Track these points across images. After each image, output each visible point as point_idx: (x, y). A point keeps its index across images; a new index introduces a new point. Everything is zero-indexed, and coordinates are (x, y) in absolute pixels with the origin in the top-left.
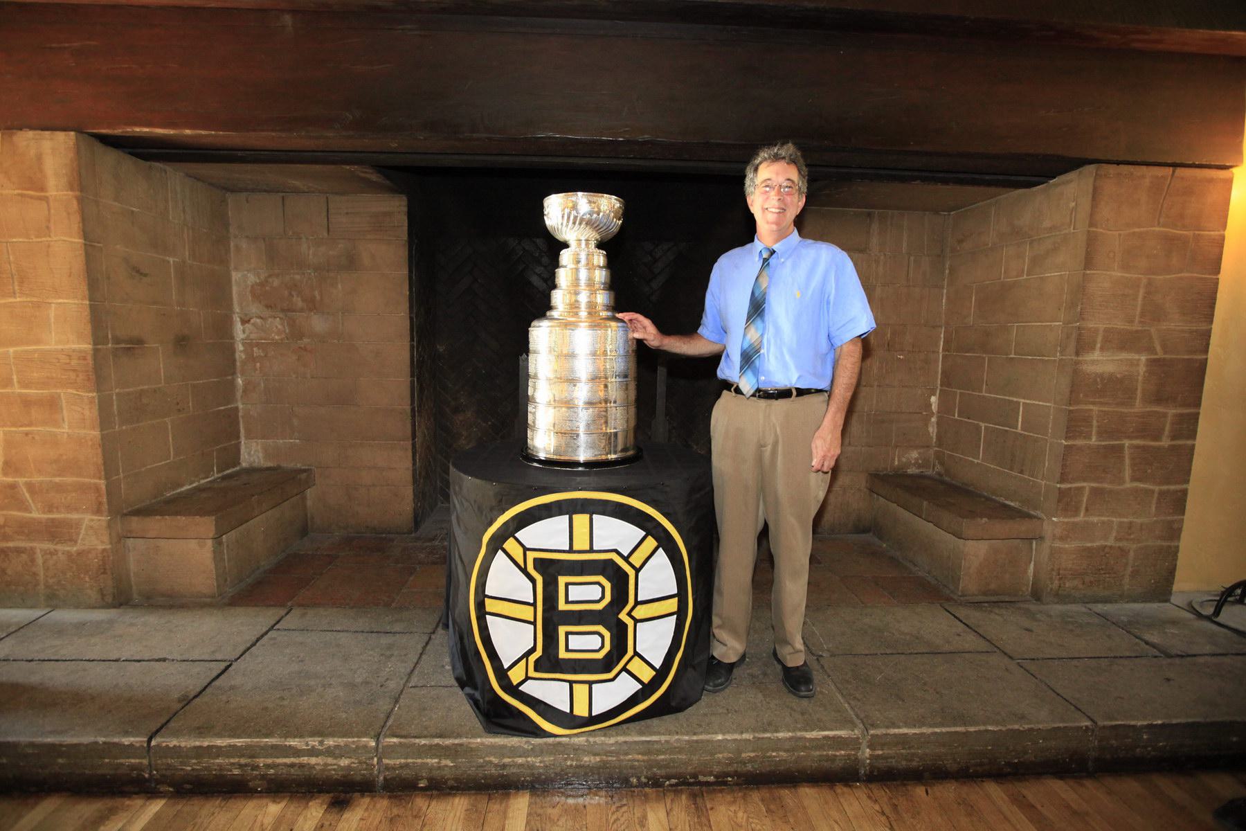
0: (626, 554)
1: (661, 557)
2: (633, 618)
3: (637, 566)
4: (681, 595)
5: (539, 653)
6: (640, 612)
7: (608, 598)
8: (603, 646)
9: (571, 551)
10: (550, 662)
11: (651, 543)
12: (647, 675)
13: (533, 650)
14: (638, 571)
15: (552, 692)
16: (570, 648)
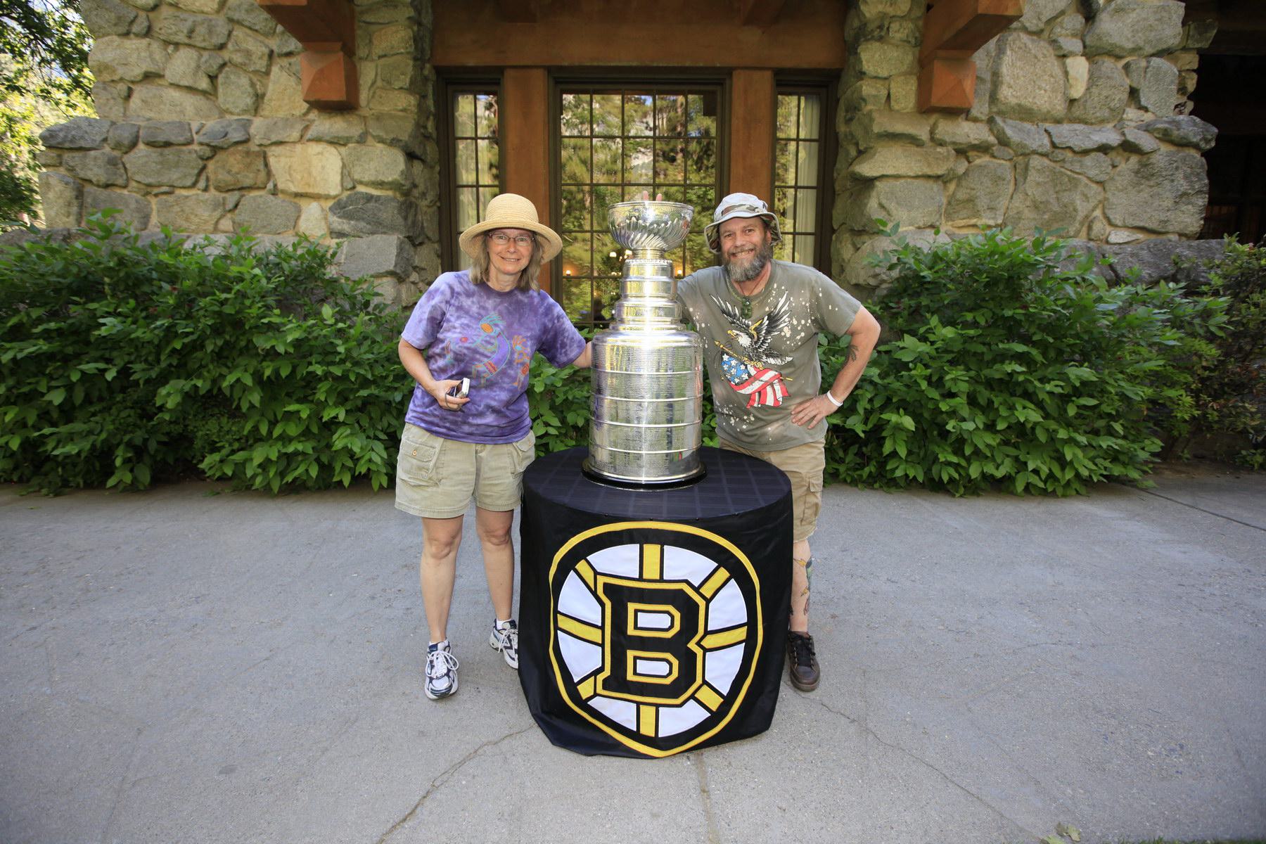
0: (696, 586)
1: (733, 588)
2: (702, 647)
3: (708, 596)
4: (751, 624)
5: (607, 672)
6: (709, 642)
7: (677, 627)
8: (670, 673)
9: (641, 579)
10: (617, 683)
11: (723, 574)
12: (714, 702)
13: (601, 669)
14: (708, 601)
15: (620, 710)
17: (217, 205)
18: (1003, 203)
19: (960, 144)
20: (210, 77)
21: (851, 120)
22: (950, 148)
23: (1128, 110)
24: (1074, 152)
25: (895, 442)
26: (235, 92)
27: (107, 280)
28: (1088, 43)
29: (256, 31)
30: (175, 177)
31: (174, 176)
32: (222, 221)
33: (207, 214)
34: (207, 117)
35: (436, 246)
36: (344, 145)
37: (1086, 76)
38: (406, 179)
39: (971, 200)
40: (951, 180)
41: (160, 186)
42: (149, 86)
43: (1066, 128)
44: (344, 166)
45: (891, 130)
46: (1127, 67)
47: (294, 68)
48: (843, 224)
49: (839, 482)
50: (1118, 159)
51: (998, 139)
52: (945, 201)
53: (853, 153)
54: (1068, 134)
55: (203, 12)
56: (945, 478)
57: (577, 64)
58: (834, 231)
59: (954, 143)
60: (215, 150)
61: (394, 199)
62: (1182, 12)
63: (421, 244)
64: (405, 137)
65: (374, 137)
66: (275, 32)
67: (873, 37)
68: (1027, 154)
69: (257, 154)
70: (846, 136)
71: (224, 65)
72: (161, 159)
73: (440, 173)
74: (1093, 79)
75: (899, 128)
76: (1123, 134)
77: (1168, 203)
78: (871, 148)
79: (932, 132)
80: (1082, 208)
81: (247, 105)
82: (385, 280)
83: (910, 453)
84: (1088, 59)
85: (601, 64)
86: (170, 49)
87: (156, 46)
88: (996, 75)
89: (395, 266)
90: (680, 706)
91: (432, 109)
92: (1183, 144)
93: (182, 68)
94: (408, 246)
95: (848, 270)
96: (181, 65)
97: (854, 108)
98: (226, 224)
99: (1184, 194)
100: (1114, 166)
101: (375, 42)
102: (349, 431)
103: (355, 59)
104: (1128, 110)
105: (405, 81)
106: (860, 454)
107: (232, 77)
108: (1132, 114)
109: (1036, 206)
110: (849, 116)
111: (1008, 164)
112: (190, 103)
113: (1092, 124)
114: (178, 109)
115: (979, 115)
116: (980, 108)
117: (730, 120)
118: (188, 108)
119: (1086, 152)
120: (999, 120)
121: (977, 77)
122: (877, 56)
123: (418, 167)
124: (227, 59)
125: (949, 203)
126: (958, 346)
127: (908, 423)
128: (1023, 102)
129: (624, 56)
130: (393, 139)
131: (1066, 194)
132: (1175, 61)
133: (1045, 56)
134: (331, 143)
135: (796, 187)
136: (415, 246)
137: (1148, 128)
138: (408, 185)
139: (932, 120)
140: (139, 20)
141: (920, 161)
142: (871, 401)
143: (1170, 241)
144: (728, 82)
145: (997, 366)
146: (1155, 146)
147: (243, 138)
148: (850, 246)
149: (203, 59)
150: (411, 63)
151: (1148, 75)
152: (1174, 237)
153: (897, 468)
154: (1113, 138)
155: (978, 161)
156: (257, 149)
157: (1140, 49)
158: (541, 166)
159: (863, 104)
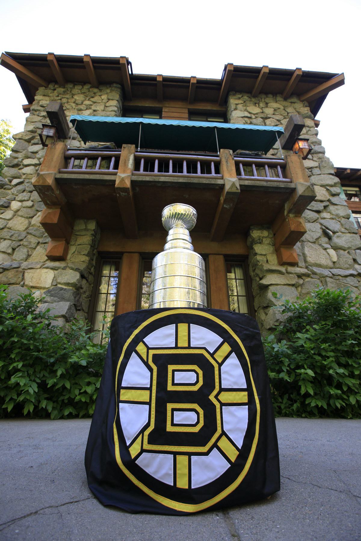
0: (212, 352)
4: (249, 389)
7: (201, 383)
11: (226, 348)
16: (175, 422)
19: (298, 273)
21: (255, 270)
24: (342, 276)
25: (306, 387)
26: (20, 254)
28: (332, 244)
29: (36, 236)
35: (86, 314)
36: (57, 270)
37: (336, 255)
38: (79, 282)
40: (298, 286)
44: (54, 277)
47: (45, 247)
48: (259, 307)
49: (283, 416)
53: (258, 279)
54: (335, 271)
55: (19, 231)
56: (339, 406)
57: (151, 252)
58: (256, 311)
61: (71, 290)
63: (79, 310)
65: (69, 267)
66: (42, 237)
67: (257, 243)
69: (21, 272)
70: (254, 275)
71: (20, 245)
73: (93, 287)
74: (338, 256)
75: (274, 268)
76: (357, 271)
78: (265, 276)
79: (286, 270)
81: (23, 258)
82: (60, 319)
83: (315, 394)
84: (334, 250)
89: (66, 313)
90: (207, 454)
91: (94, 264)
94: (73, 308)
95: (265, 323)
97: (255, 265)
101: (78, 240)
102: (21, 375)
103: (69, 245)
104: (355, 265)
105: (86, 252)
106: (290, 399)
108: (357, 266)
110: (254, 268)
111: (318, 280)
113: (344, 269)
115: (302, 266)
116: (301, 263)
119: (346, 276)
123: (84, 281)
124: (21, 244)
125: (300, 295)
126: (322, 337)
127: (310, 373)
128: (317, 262)
130: (77, 268)
133: (319, 249)
136: (77, 310)
138: (79, 285)
139: (286, 266)
141: (284, 279)
142: (289, 366)
144: (207, 259)
145: (344, 343)
148: (264, 314)
149: (13, 244)
150: (90, 247)
151: (357, 255)
153: (311, 402)
154: (355, 273)
155: (307, 280)
156: (22, 270)
157: (351, 248)
158: (134, 285)
159: (258, 263)
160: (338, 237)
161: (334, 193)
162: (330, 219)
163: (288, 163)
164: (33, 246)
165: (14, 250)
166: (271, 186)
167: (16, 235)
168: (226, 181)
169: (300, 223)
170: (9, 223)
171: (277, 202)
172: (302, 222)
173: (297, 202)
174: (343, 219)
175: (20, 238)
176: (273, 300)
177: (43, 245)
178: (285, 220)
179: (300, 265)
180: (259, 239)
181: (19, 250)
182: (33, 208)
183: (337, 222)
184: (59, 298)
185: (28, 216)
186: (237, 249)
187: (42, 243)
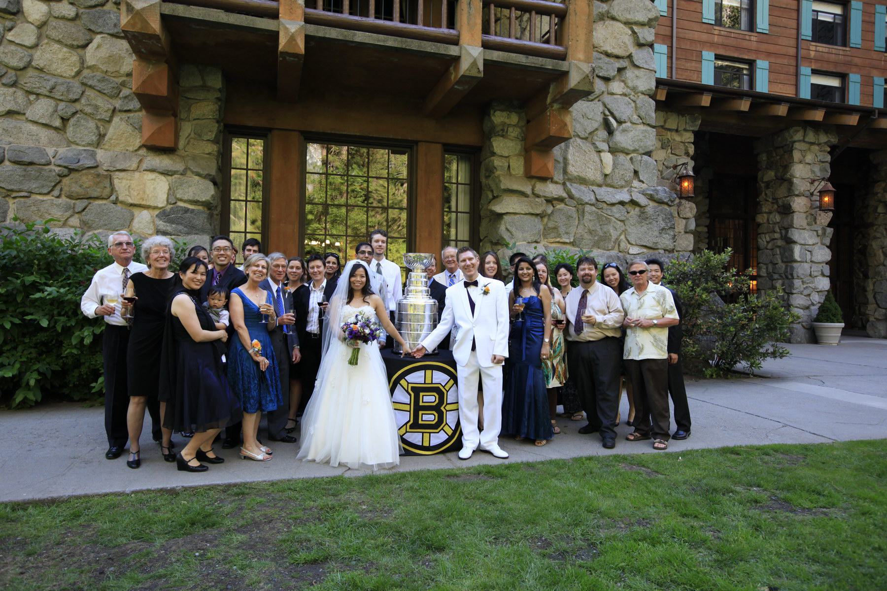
17: (68, 208)
18: (573, 230)
20: (62, 118)
21: (489, 176)
22: (543, 199)
23: (634, 181)
27: (36, 261)
28: (610, 144)
29: (104, 94)
30: (34, 186)
31: (33, 185)
32: (72, 219)
33: (60, 214)
34: (58, 146)
37: (611, 163)
39: (555, 228)
41: (20, 191)
42: (10, 120)
43: (604, 189)
44: (170, 189)
45: (510, 188)
46: (631, 159)
47: (131, 121)
50: (629, 208)
51: (567, 194)
52: (542, 227)
53: (491, 197)
55: (61, 76)
57: (321, 131)
59: (545, 197)
60: (71, 170)
62: (655, 134)
64: (213, 172)
65: (193, 172)
67: (499, 135)
68: (584, 204)
69: (106, 177)
71: (76, 113)
72: (24, 173)
74: (615, 165)
75: (515, 187)
76: (631, 196)
77: (656, 233)
79: (533, 190)
80: (614, 234)
85: (337, 132)
86: (32, 97)
87: (20, 94)
88: (565, 159)
92: (660, 202)
93: (41, 111)
96: (41, 109)
97: (491, 170)
98: (75, 221)
99: (663, 229)
100: (628, 213)
101: (192, 110)
104: (634, 181)
105: (212, 136)
107: (82, 121)
108: (636, 183)
109: (590, 232)
112: (44, 135)
114: (34, 138)
116: (558, 176)
117: (417, 171)
118: (43, 138)
119: (613, 204)
120: (568, 184)
121: (556, 160)
122: (501, 145)
125: (545, 229)
128: (580, 174)
129: (353, 130)
131: (605, 226)
132: (681, 135)
133: (589, 151)
134: (162, 173)
135: (457, 212)
137: (644, 193)
139: (533, 181)
140: (8, 75)
143: (659, 253)
144: (415, 148)
146: (647, 203)
147: (95, 165)
152: (662, 251)
154: (626, 197)
155: (558, 207)
156: (106, 173)
160: (624, 131)
161: (642, 41)
162: (621, 95)
163: (570, 15)
164: (106, 116)
165: (65, 120)
166: (533, 65)
167: (62, 88)
168: (463, 52)
169: (566, 125)
170: (36, 57)
171: (540, 80)
172: (568, 124)
173: (565, 94)
174: (642, 96)
175: (72, 96)
176: (506, 236)
177: (125, 115)
178: (545, 109)
179: (556, 179)
180: (503, 130)
181: (78, 123)
182: (78, 22)
183: (631, 101)
184: (186, 227)
185: (75, 43)
186: (465, 136)
187: (120, 111)
